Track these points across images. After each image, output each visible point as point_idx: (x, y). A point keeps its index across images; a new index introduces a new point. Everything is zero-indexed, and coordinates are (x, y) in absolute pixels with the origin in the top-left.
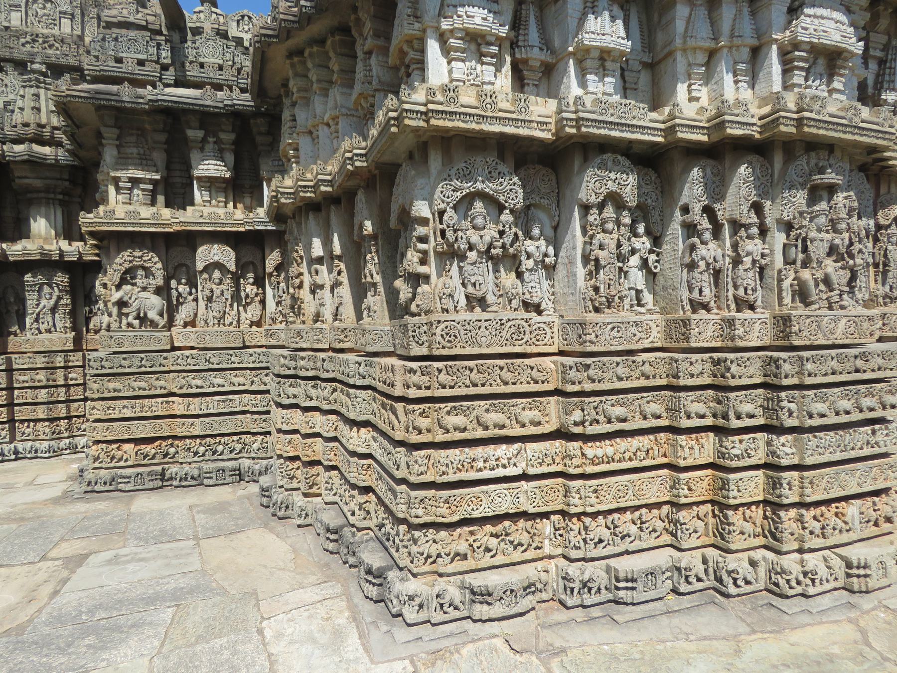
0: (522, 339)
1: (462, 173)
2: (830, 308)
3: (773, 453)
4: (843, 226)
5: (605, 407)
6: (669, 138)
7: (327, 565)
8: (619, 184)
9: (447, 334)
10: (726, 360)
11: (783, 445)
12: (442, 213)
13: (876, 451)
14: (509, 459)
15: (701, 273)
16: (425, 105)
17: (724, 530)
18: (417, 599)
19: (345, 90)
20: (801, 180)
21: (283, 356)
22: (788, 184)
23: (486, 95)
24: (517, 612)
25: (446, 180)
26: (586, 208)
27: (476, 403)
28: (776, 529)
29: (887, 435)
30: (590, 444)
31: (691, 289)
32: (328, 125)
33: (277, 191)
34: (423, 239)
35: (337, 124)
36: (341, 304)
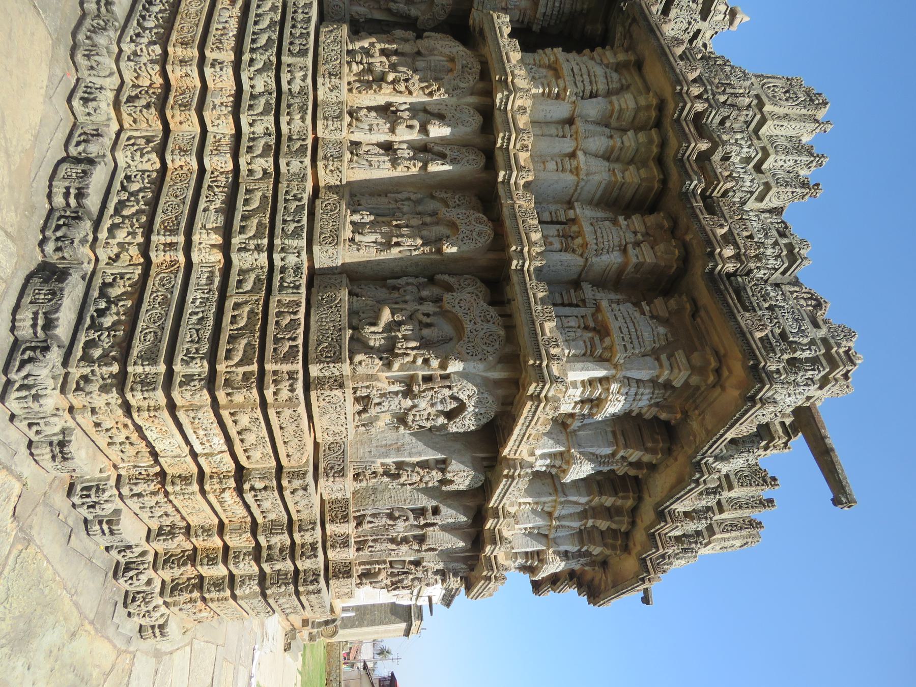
3: (243, 582)
6: (490, 511)
7: (33, 208)
10: (316, 556)
16: (546, 396)
17: (173, 563)
18: (36, 404)
19: (603, 185)
21: (305, 76)
26: (442, 465)
28: (181, 590)
30: (234, 493)
31: (374, 515)
32: (573, 155)
33: (511, 93)
34: (426, 361)
35: (571, 171)
36: (371, 165)
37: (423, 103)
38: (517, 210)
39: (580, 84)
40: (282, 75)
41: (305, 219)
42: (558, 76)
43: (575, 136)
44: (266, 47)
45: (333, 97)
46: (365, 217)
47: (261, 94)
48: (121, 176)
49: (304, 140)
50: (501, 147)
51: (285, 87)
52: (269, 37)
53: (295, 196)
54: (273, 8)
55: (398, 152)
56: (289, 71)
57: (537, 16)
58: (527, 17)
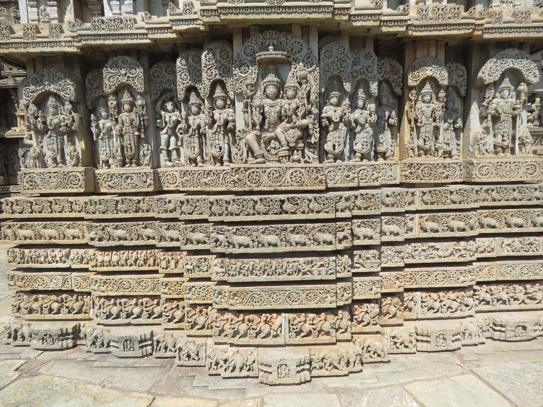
0: (78, 184)
1: (35, 81)
2: (279, 161)
4: (290, 93)
5: (109, 229)
8: (128, 77)
9: (30, 181)
11: (216, 265)
12: (27, 107)
13: (309, 277)
14: (61, 258)
15: (190, 137)
20: (250, 58)
22: (238, 63)
23: (28, 29)
24: (54, 348)
25: (26, 86)
27: (36, 223)
29: (322, 265)
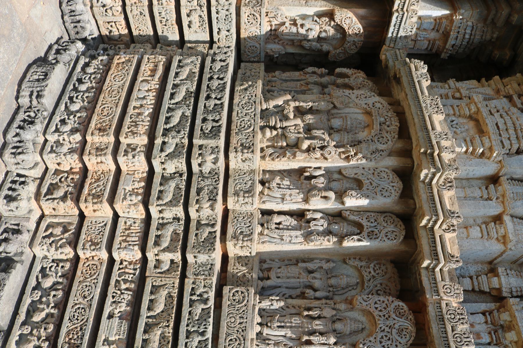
32: (498, 219)
33: (438, 170)
37: (339, 167)
38: (444, 311)
39: (507, 143)
40: (192, 161)
41: (210, 329)
42: (481, 132)
43: (502, 199)
44: (177, 129)
45: (245, 166)
46: (275, 303)
47: (172, 177)
48: (37, 268)
49: (213, 225)
50: (425, 226)
51: (195, 168)
52: (183, 113)
53: (200, 295)
54: (191, 74)
55: (311, 224)
56: (200, 155)
57: (447, 47)
58: (436, 47)
